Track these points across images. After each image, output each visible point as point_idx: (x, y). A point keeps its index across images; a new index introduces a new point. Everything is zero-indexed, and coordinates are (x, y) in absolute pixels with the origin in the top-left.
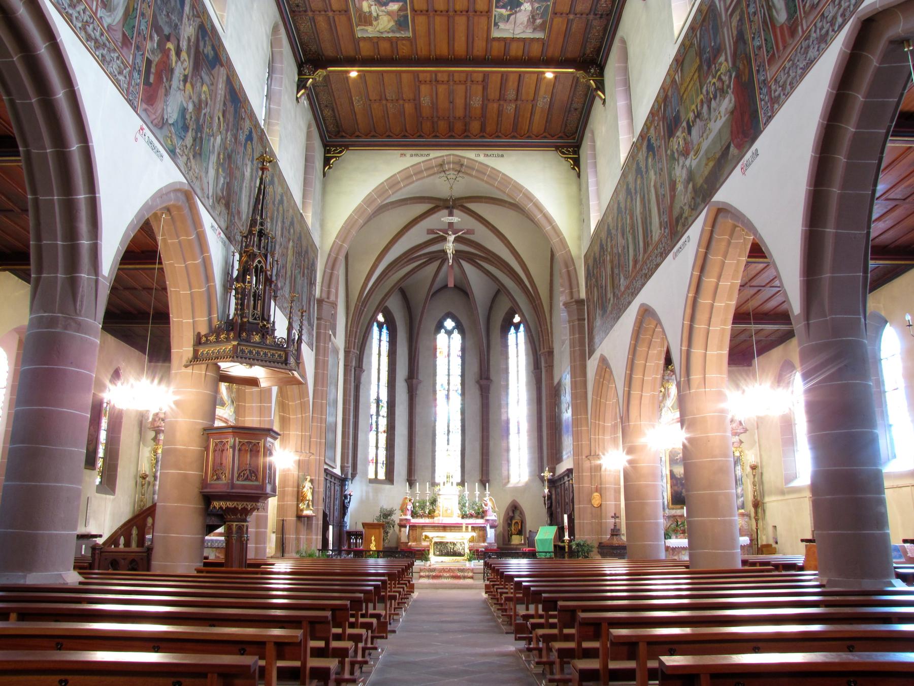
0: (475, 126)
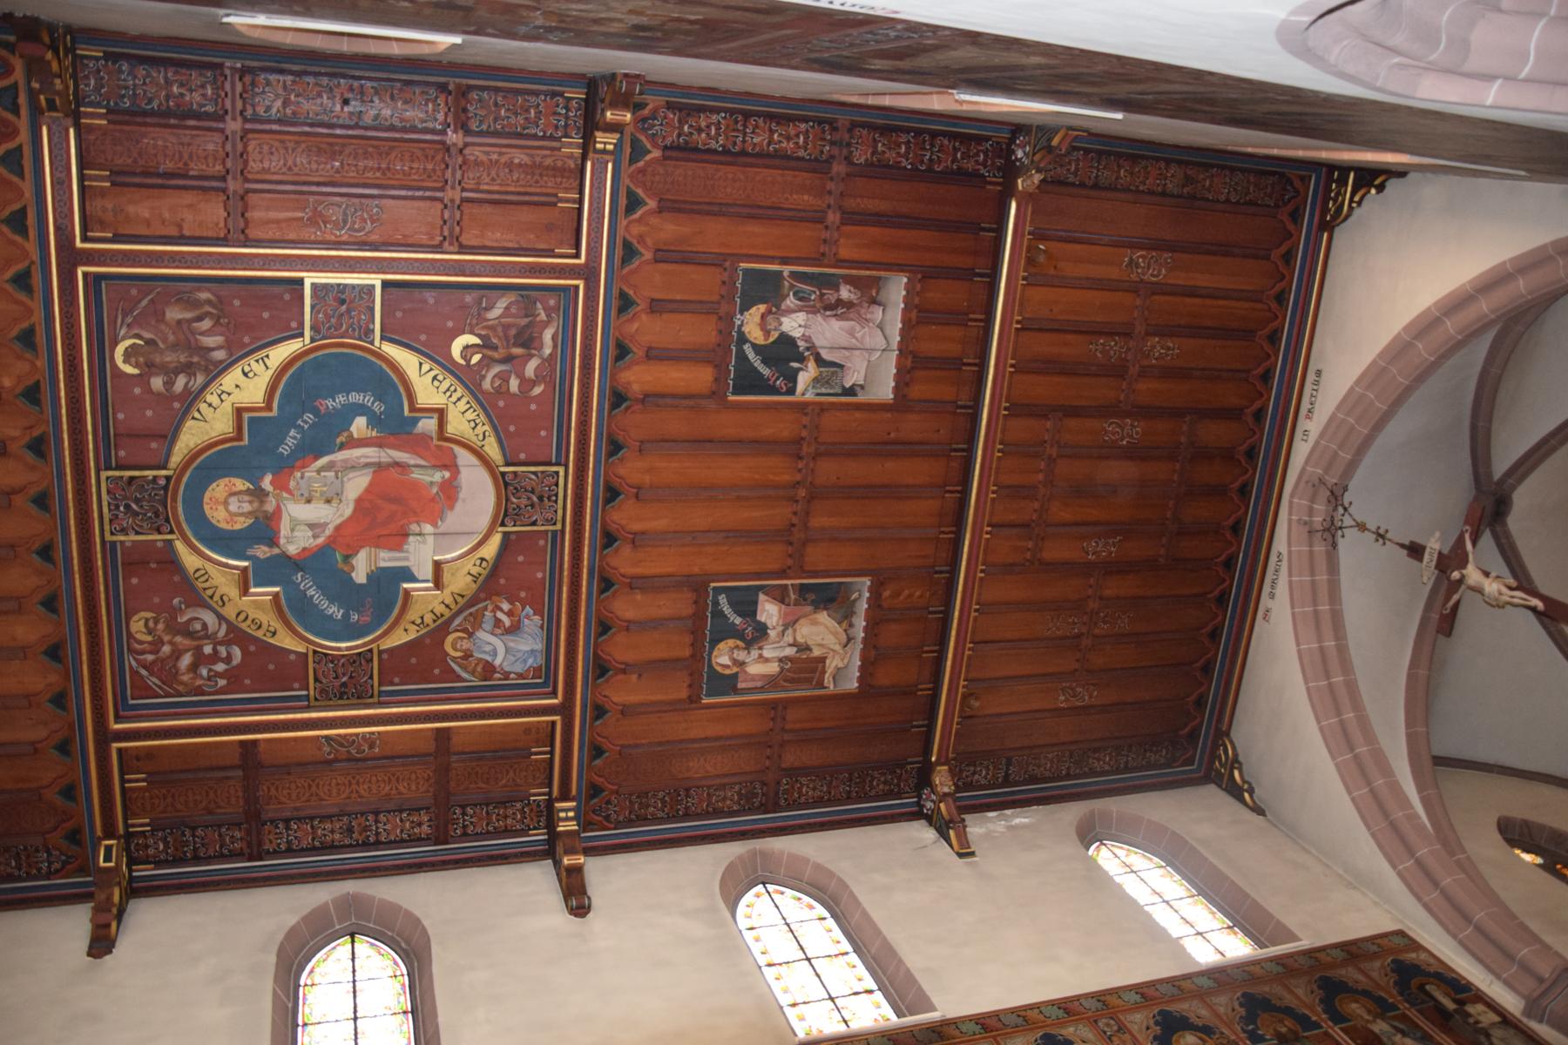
0: (1214, 433)
